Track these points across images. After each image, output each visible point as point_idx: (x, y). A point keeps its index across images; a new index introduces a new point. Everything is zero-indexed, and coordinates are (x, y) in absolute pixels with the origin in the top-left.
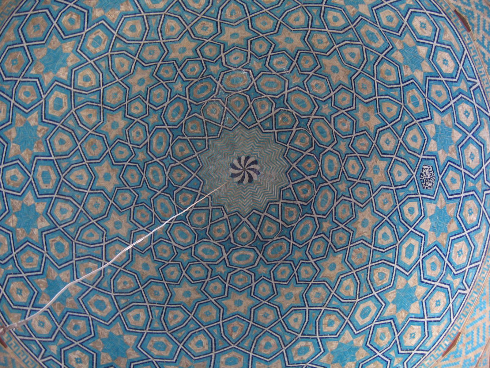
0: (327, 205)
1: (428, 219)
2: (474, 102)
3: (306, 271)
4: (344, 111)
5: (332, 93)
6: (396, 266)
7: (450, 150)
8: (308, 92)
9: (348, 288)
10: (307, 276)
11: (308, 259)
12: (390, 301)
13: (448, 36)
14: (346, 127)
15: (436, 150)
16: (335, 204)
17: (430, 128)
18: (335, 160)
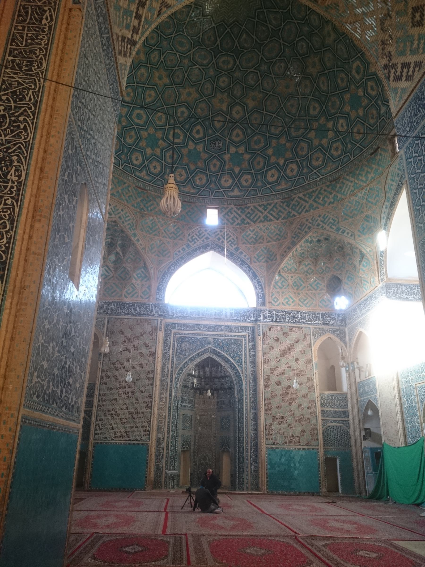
0: (199, 60)
1: (194, 146)
2: (251, 189)
3: (156, 56)
4: (260, 81)
5: (273, 76)
6: (167, 127)
7: (230, 163)
8: (277, 58)
9: (150, 96)
10: (152, 59)
11: (163, 54)
12: (149, 132)
13: (283, 186)
14: (250, 80)
15: (231, 152)
16: (200, 67)
17: (242, 150)
18: (229, 67)
